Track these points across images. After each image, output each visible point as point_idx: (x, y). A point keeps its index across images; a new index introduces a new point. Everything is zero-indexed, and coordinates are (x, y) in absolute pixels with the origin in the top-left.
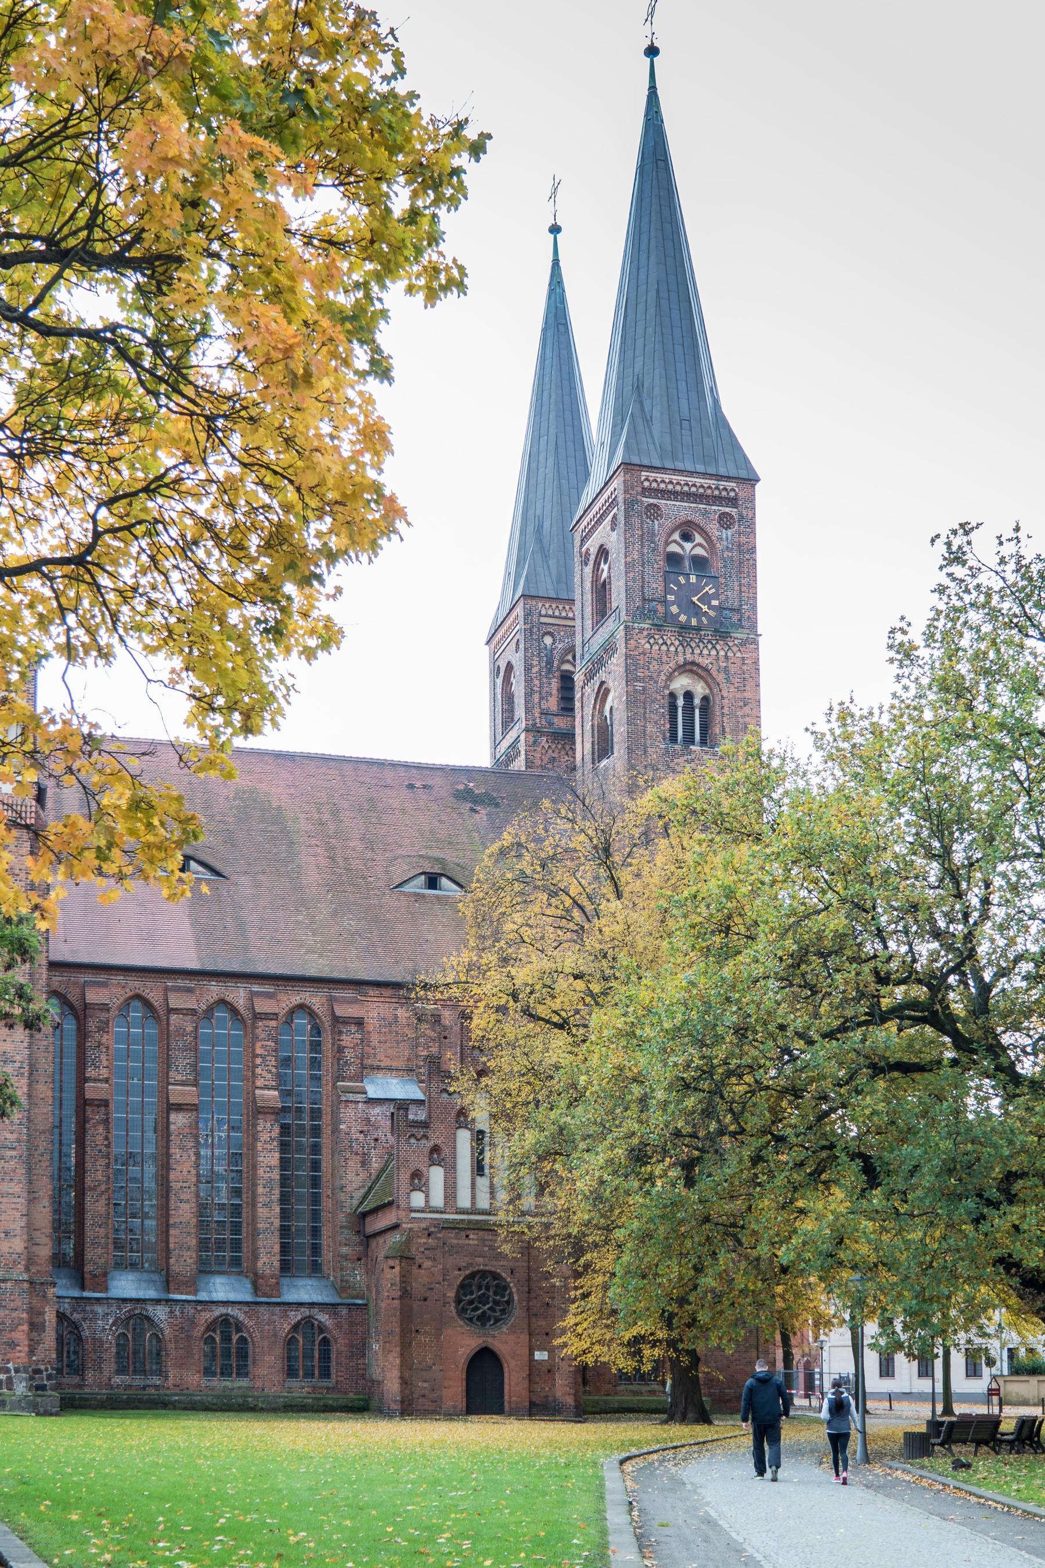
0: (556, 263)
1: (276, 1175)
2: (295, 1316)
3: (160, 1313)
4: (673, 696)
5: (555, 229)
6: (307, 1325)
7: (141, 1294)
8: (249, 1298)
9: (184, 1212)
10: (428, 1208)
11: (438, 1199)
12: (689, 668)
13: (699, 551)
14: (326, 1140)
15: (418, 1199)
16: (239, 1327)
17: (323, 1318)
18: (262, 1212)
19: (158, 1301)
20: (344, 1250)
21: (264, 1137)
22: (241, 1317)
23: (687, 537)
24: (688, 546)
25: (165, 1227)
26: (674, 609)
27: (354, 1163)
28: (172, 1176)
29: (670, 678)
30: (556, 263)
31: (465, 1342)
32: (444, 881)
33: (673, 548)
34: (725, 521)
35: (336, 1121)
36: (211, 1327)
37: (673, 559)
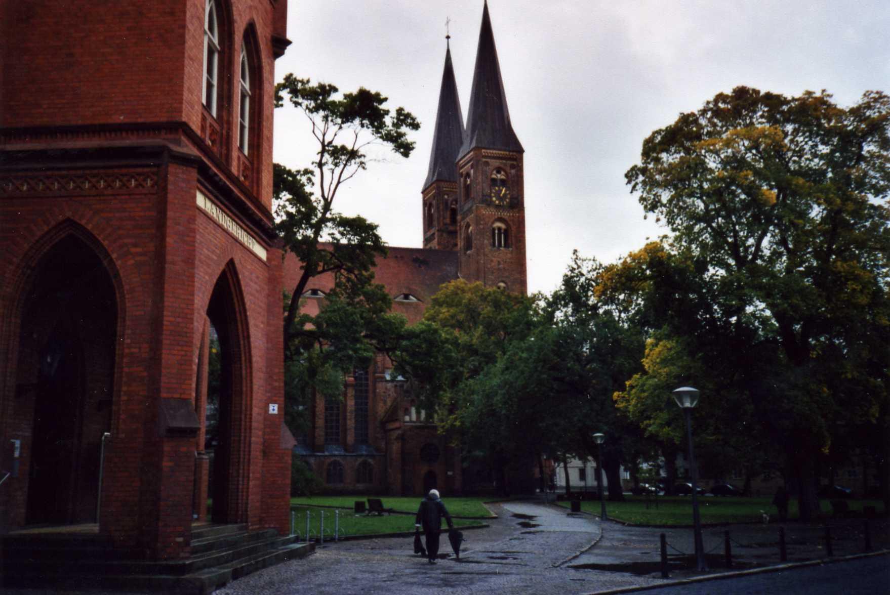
0: (448, 52)
1: (353, 408)
2: (360, 460)
3: (312, 461)
4: (494, 230)
5: (448, 37)
6: (365, 464)
7: (304, 453)
8: (342, 453)
9: (320, 422)
10: (411, 421)
11: (414, 417)
12: (500, 219)
13: (503, 177)
14: (371, 395)
15: (407, 418)
16: (340, 464)
17: (370, 460)
18: (348, 422)
19: (310, 456)
20: (277, 384)
21: (349, 395)
22: (341, 461)
23: (499, 172)
24: (499, 176)
25: (314, 427)
26: (494, 199)
27: (381, 404)
28: (317, 409)
29: (493, 223)
30: (448, 52)
31: (424, 469)
32: (411, 297)
33: (494, 176)
34: (512, 167)
35: (375, 388)
36: (330, 465)
37: (494, 181)
